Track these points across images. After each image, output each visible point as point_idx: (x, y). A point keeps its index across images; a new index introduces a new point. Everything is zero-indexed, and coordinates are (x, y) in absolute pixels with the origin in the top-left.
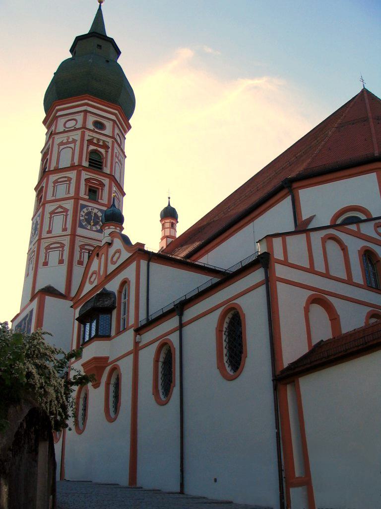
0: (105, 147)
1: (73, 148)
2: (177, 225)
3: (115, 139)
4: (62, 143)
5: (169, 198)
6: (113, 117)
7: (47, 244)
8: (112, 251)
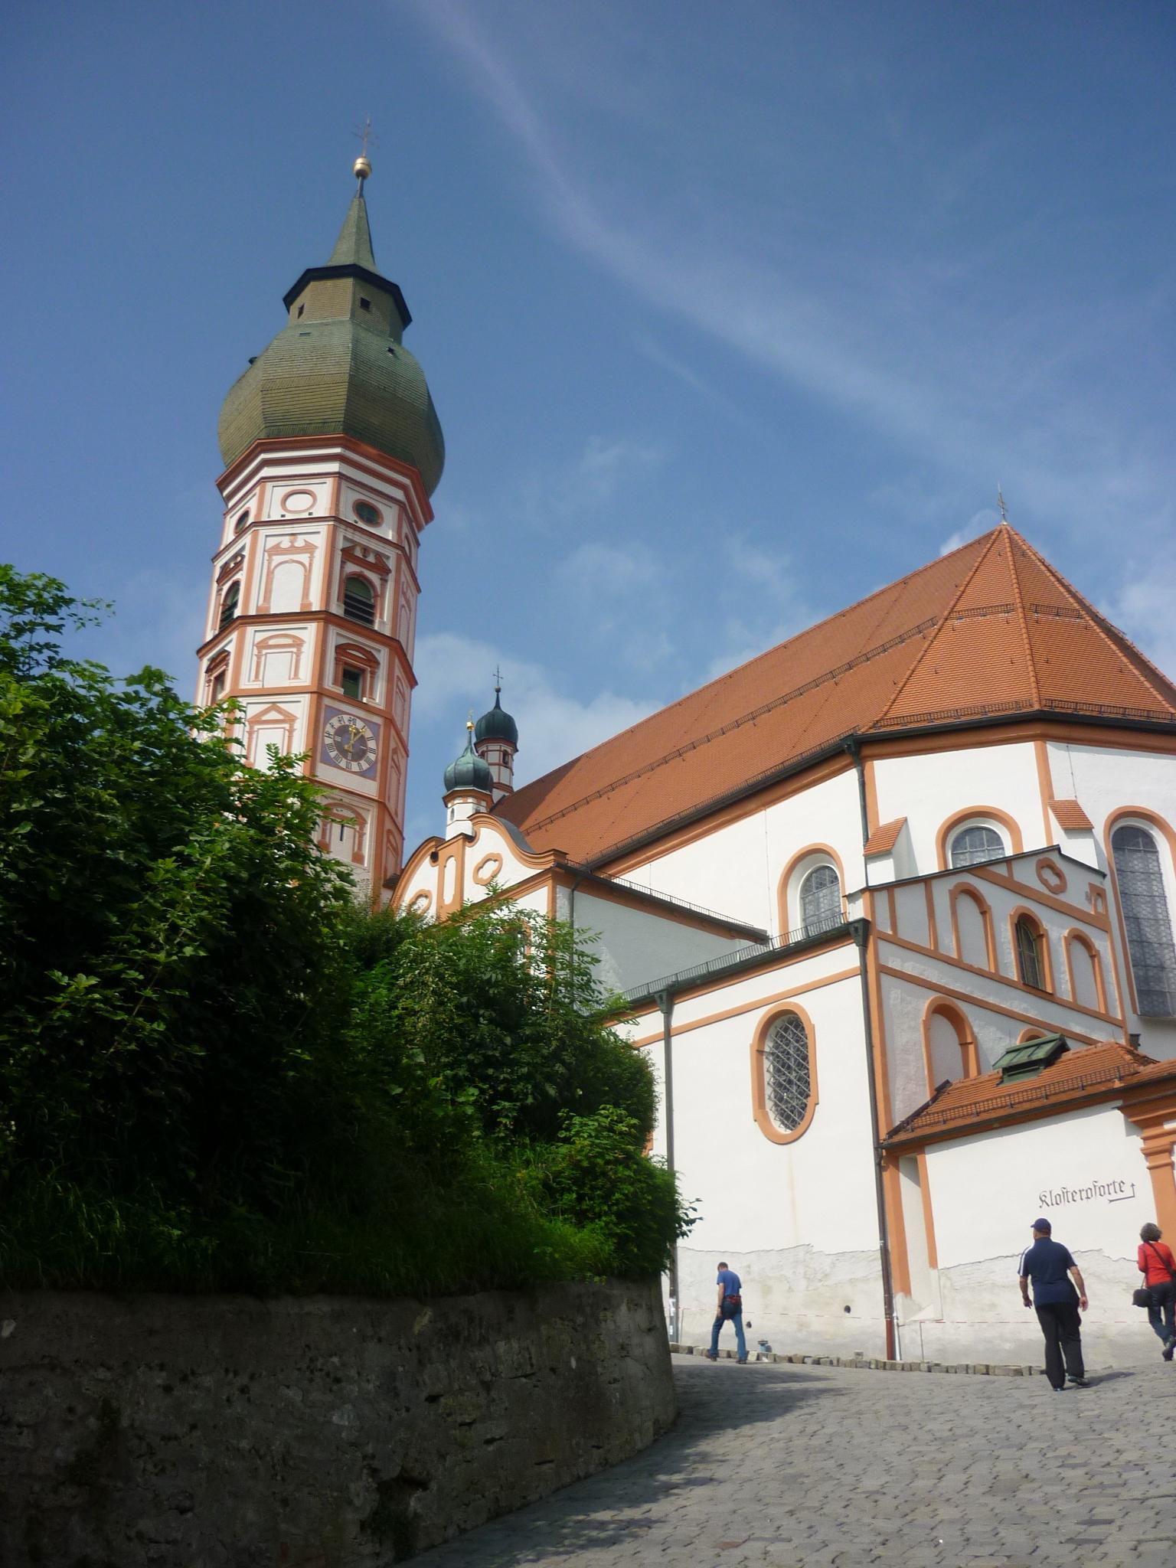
0: (382, 570)
1: (307, 565)
2: (516, 756)
3: (402, 549)
4: (277, 550)
5: (498, 691)
6: (399, 494)
8: (473, 855)
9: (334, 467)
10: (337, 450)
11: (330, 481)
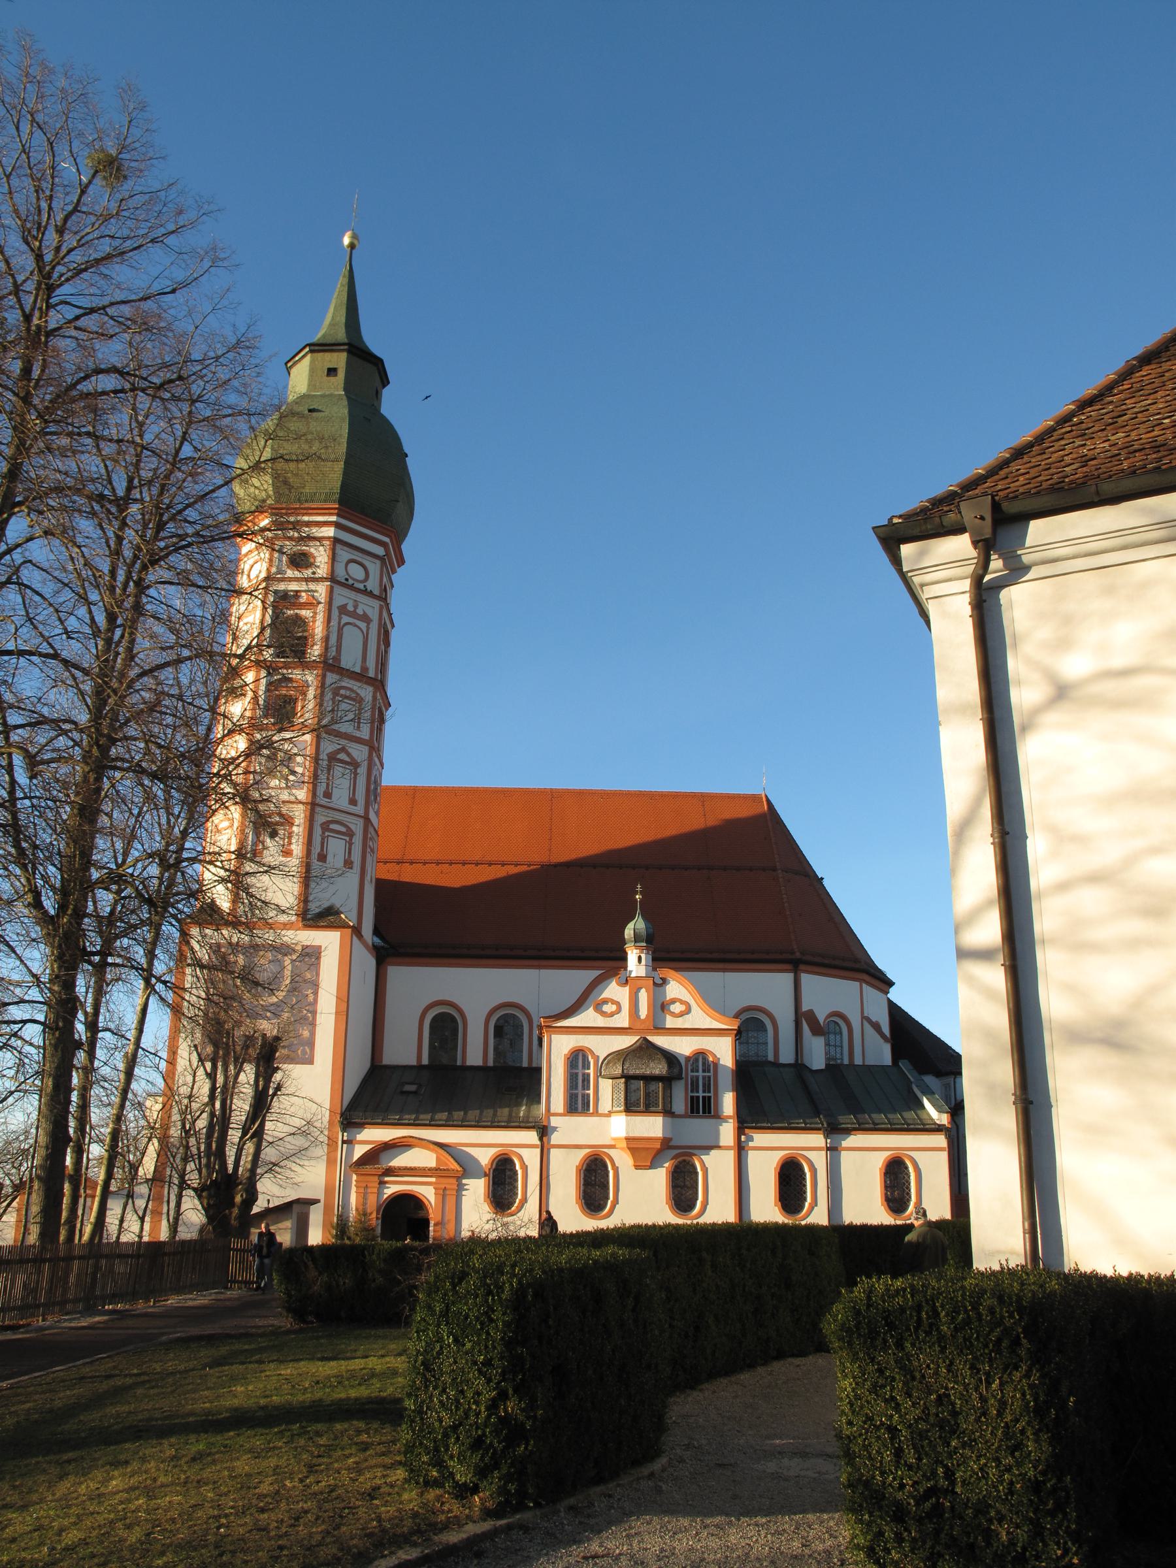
4: (343, 610)
7: (324, 819)
9: (380, 551)
11: (378, 562)
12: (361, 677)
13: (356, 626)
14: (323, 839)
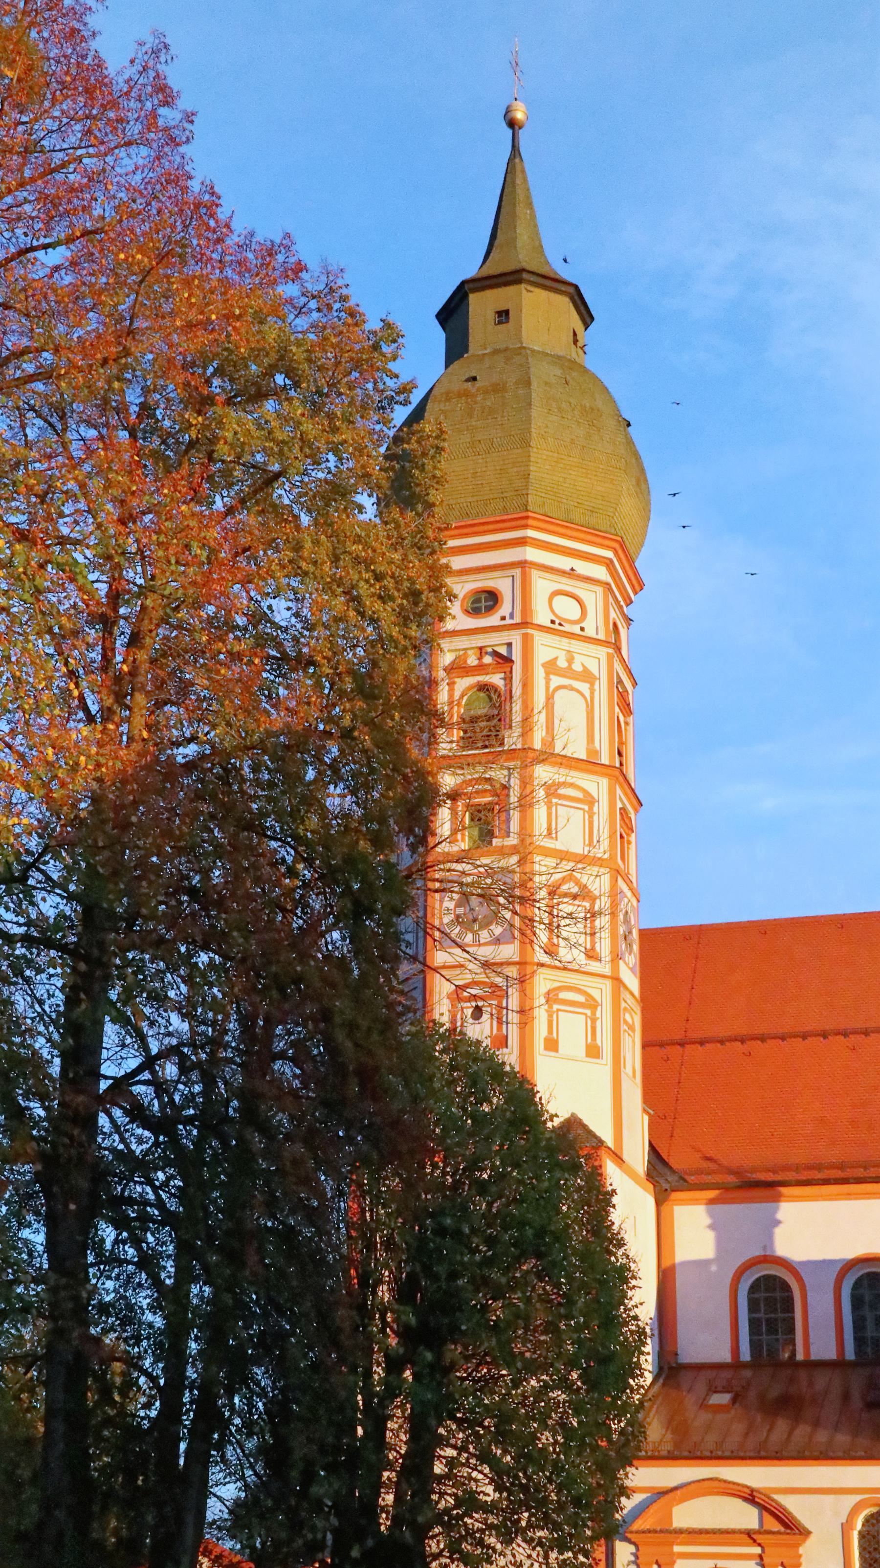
4: (551, 667)
7: (550, 985)
9: (600, 572)
10: (609, 554)
12: (590, 765)
13: (571, 688)
14: (550, 1016)
